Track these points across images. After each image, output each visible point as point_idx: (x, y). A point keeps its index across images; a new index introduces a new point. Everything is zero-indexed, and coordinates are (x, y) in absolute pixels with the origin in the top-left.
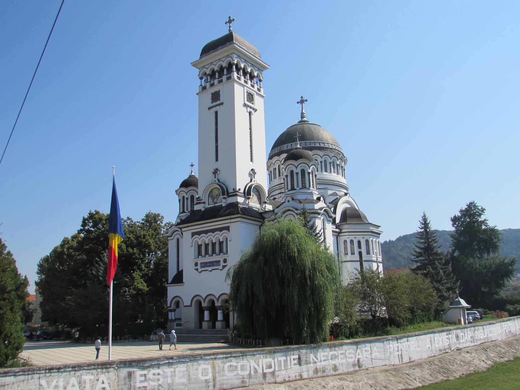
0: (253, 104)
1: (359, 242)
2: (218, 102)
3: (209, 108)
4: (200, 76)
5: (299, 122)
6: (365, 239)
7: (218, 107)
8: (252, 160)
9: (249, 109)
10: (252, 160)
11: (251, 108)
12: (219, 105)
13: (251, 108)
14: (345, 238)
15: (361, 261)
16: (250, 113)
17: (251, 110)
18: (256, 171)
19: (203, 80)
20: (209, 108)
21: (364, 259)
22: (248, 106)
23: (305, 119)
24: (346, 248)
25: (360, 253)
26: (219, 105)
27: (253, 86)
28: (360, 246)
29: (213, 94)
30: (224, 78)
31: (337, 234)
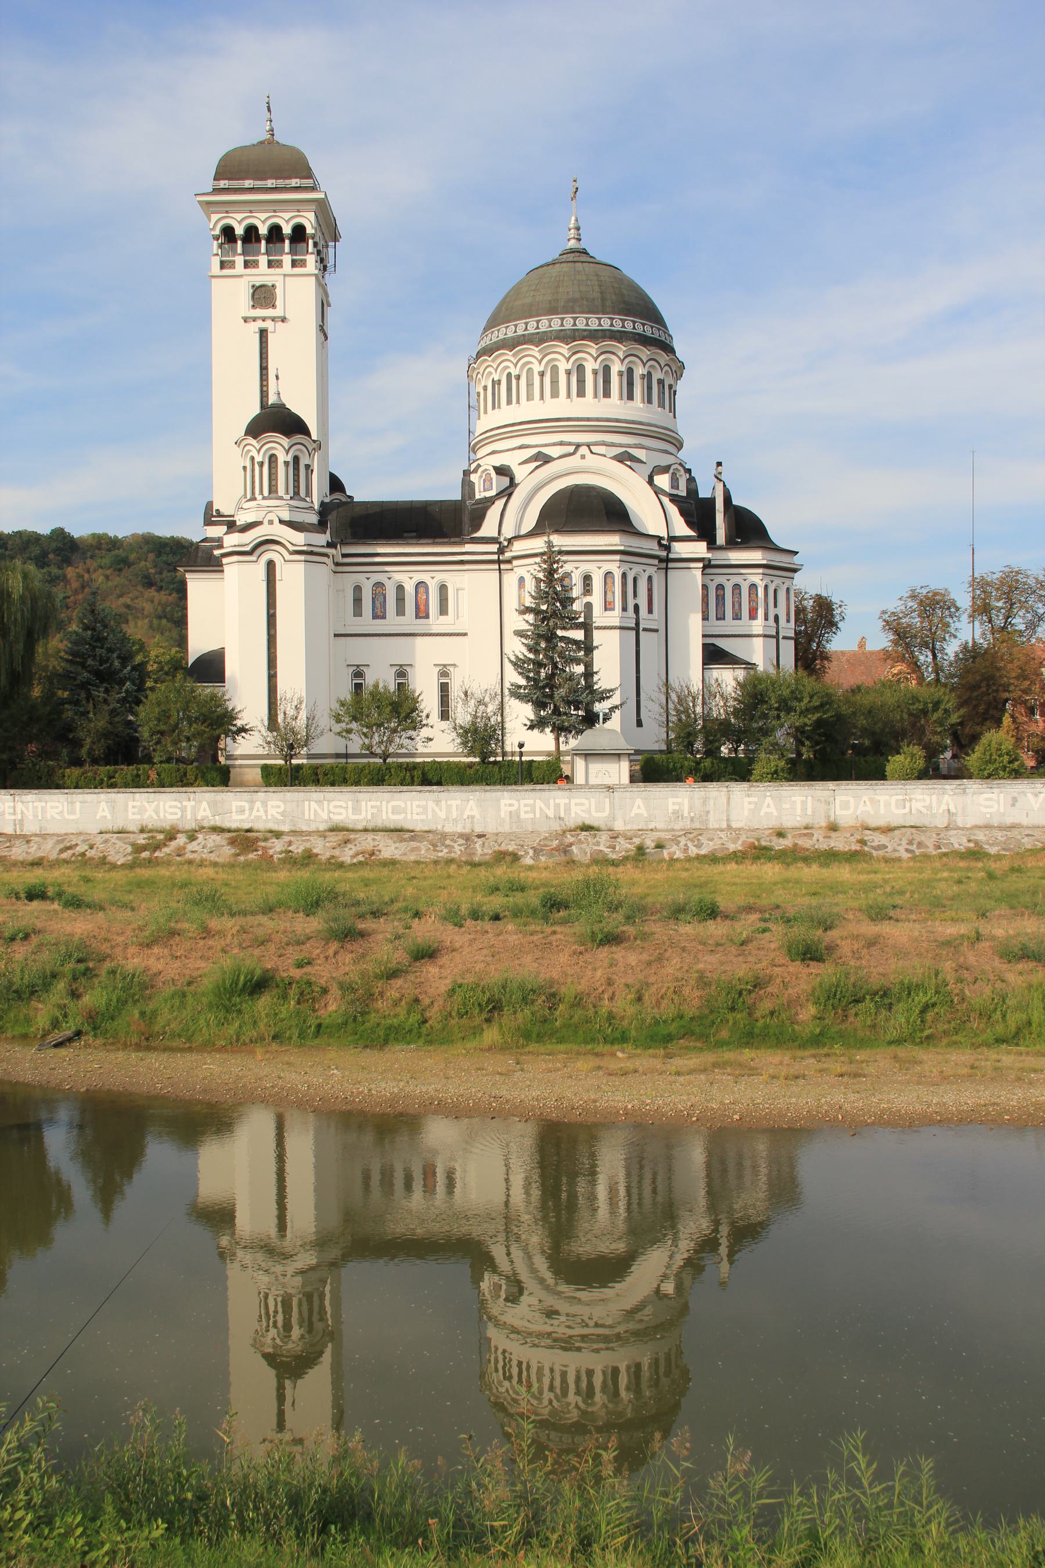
0: (274, 306)
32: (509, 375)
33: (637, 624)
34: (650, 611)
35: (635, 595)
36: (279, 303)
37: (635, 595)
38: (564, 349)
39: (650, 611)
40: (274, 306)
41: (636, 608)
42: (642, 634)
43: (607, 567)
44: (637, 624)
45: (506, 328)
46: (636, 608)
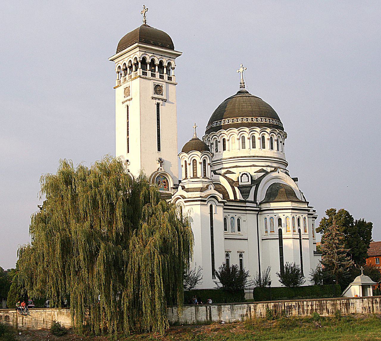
0: (162, 95)
1: (280, 220)
2: (129, 98)
3: (123, 103)
4: (117, 71)
5: (239, 92)
6: (297, 216)
7: (128, 102)
8: (159, 150)
9: (158, 101)
10: (159, 150)
11: (159, 99)
12: (129, 100)
13: (159, 99)
14: (266, 216)
15: (281, 239)
16: (158, 105)
17: (160, 102)
18: (163, 158)
19: (120, 74)
20: (123, 103)
21: (284, 236)
22: (156, 98)
23: (246, 89)
24: (266, 227)
25: (280, 230)
26: (129, 100)
27: (162, 77)
28: (280, 224)
29: (125, 89)
30: (133, 74)
31: (257, 213)
32: (217, 140)
33: (300, 237)
34: (305, 231)
35: (299, 225)
36: (164, 93)
37: (299, 225)
38: (247, 129)
39: (305, 231)
40: (162, 95)
41: (299, 230)
42: (302, 240)
43: (286, 215)
44: (300, 237)
45: (220, 122)
46: (299, 230)
